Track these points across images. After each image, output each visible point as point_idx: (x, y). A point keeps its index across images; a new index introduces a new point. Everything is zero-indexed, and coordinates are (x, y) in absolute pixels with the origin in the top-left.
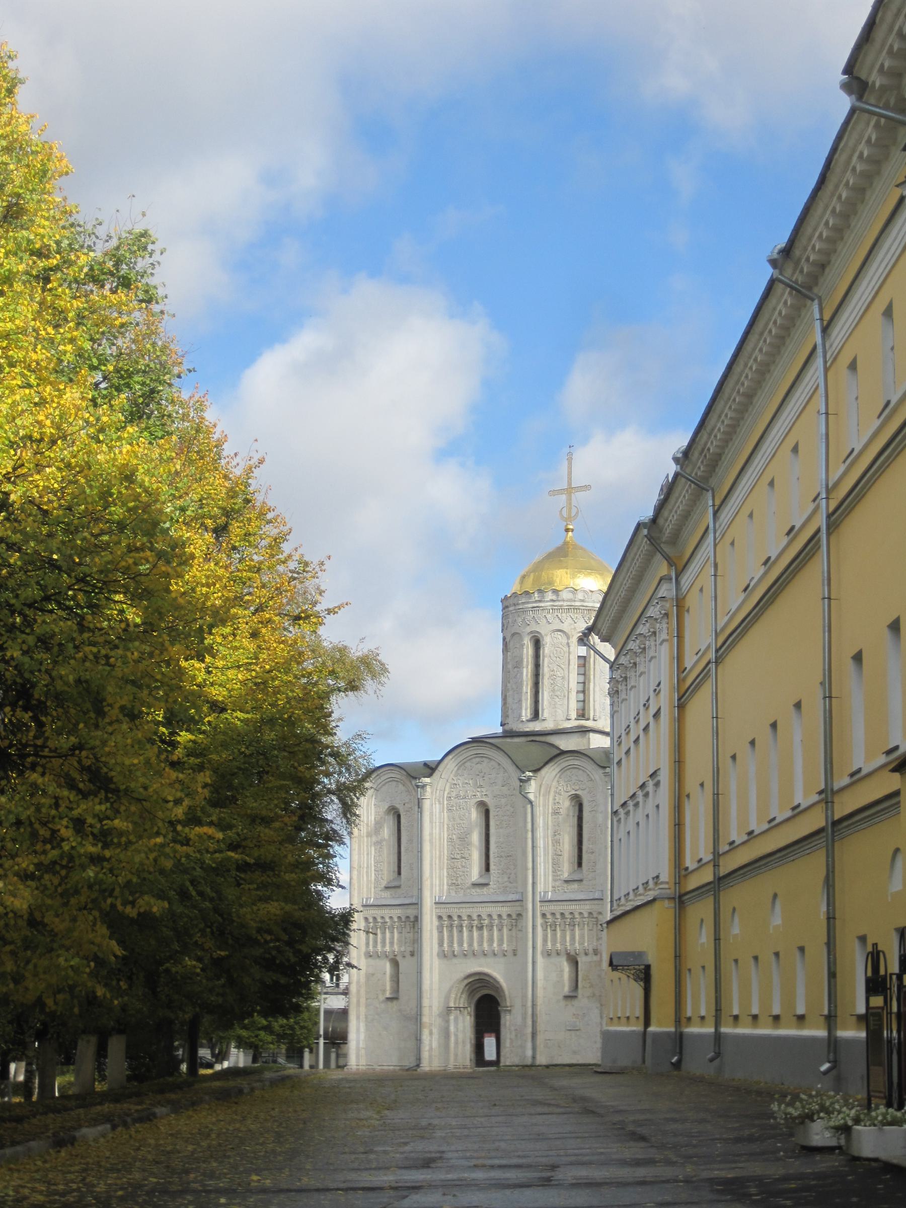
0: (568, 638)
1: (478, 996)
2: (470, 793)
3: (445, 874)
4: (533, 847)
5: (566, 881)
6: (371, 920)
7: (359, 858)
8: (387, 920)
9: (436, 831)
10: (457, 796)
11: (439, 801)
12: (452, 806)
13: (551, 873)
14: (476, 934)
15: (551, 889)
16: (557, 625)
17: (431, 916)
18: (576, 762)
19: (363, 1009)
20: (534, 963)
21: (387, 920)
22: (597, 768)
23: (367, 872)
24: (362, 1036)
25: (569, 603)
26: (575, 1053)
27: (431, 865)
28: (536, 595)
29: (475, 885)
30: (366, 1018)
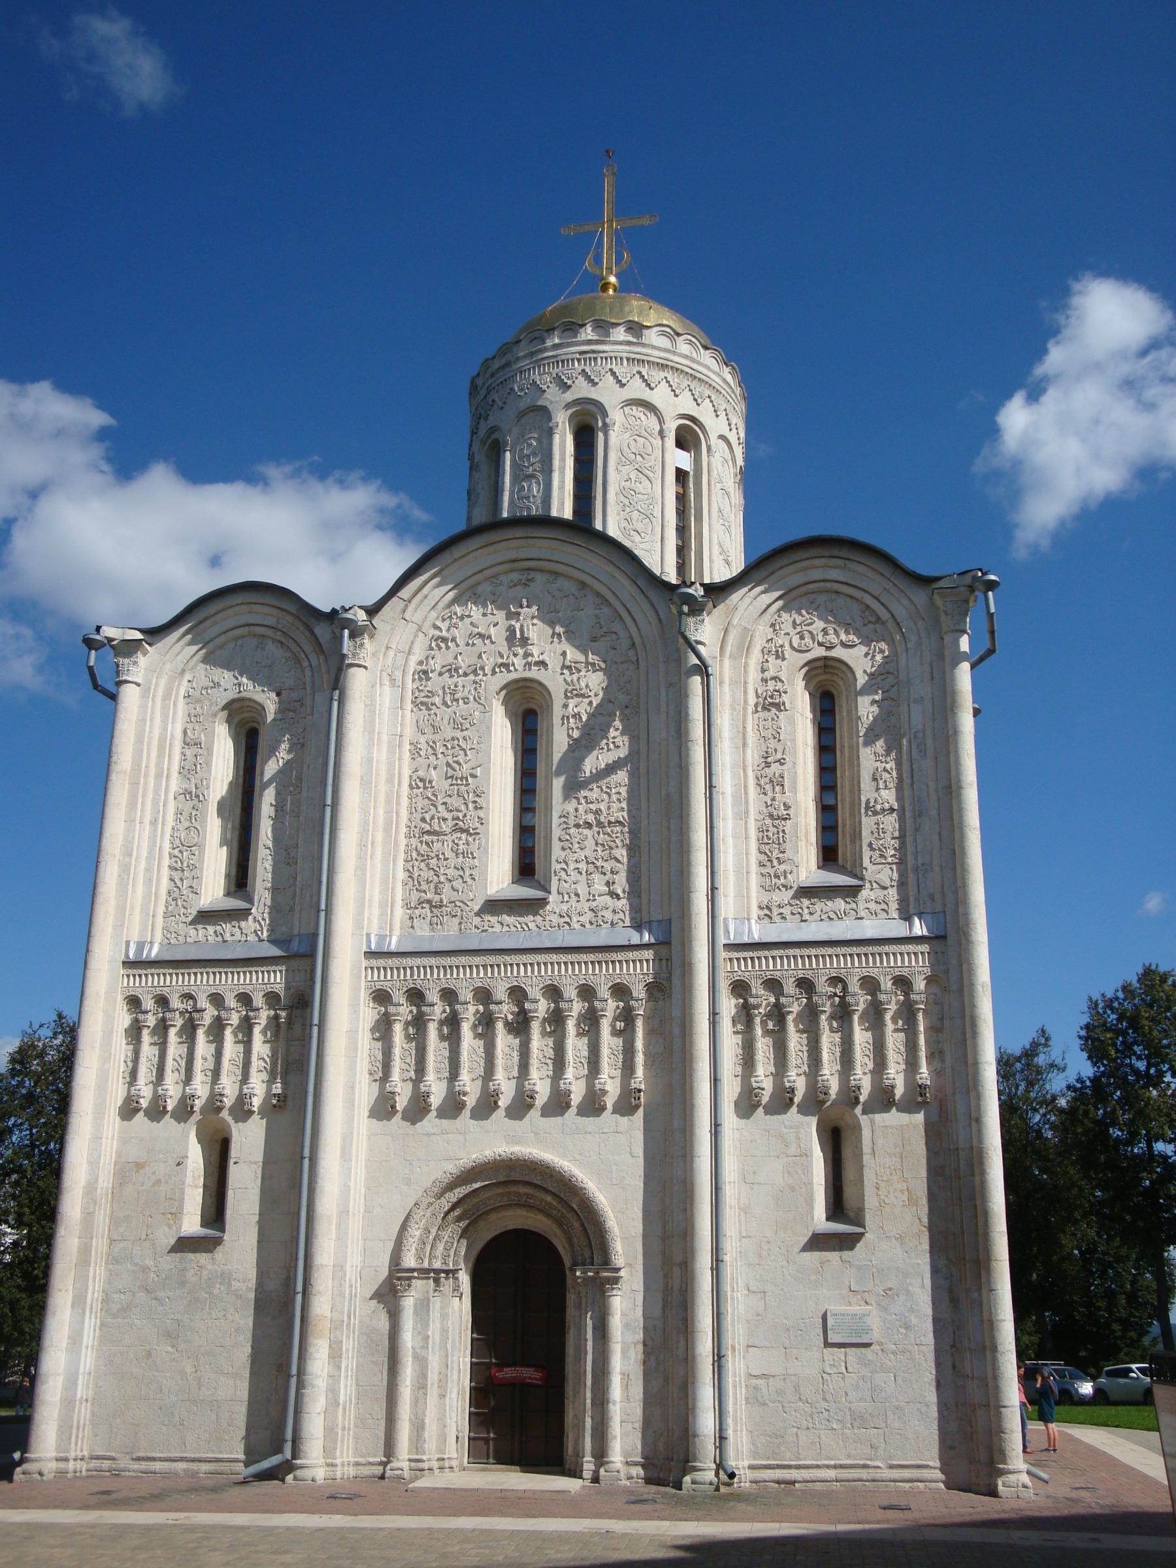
0: (661, 421)
1: (487, 1233)
2: (489, 662)
3: (401, 875)
4: (710, 787)
5: (806, 892)
6: (148, 1003)
7: (130, 830)
8: (203, 1002)
9: (381, 755)
10: (452, 670)
11: (393, 681)
12: (432, 693)
13: (754, 867)
14: (504, 1041)
15: (755, 912)
16: (636, 389)
17: (355, 989)
18: (834, 574)
19: (97, 1275)
20: (716, 1128)
21: (203, 1002)
22: (903, 583)
23: (148, 870)
24: (88, 1360)
25: (662, 354)
26: (859, 1420)
27: (362, 846)
28: (589, 329)
29: (494, 906)
30: (106, 1300)
